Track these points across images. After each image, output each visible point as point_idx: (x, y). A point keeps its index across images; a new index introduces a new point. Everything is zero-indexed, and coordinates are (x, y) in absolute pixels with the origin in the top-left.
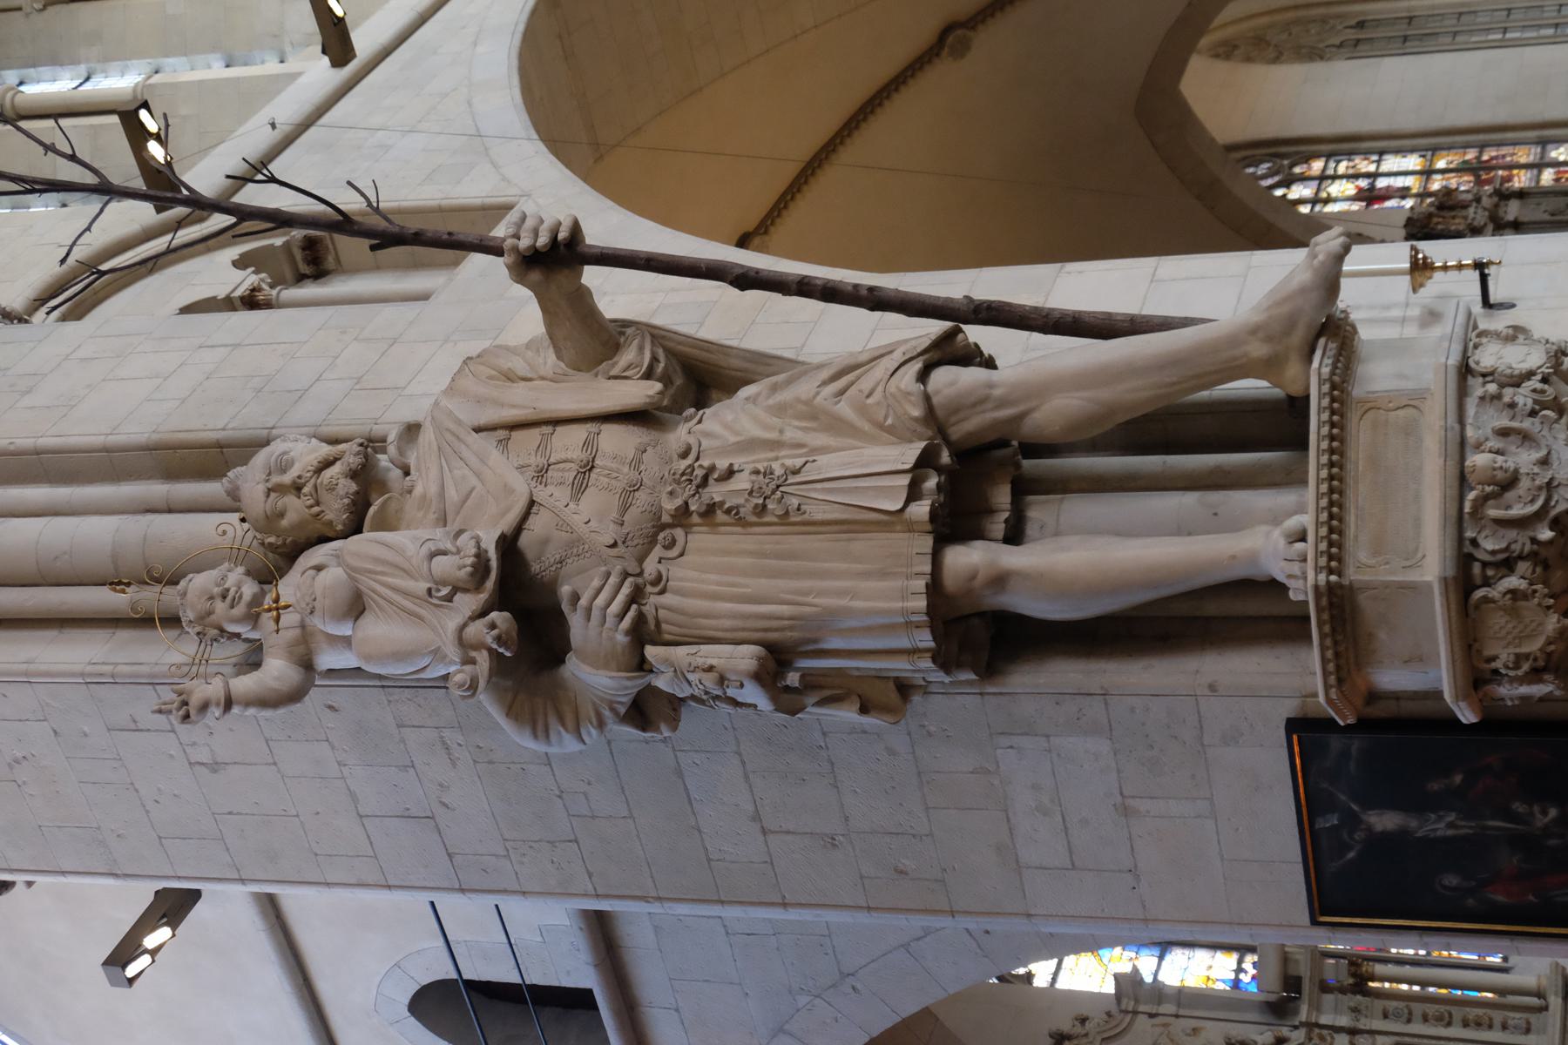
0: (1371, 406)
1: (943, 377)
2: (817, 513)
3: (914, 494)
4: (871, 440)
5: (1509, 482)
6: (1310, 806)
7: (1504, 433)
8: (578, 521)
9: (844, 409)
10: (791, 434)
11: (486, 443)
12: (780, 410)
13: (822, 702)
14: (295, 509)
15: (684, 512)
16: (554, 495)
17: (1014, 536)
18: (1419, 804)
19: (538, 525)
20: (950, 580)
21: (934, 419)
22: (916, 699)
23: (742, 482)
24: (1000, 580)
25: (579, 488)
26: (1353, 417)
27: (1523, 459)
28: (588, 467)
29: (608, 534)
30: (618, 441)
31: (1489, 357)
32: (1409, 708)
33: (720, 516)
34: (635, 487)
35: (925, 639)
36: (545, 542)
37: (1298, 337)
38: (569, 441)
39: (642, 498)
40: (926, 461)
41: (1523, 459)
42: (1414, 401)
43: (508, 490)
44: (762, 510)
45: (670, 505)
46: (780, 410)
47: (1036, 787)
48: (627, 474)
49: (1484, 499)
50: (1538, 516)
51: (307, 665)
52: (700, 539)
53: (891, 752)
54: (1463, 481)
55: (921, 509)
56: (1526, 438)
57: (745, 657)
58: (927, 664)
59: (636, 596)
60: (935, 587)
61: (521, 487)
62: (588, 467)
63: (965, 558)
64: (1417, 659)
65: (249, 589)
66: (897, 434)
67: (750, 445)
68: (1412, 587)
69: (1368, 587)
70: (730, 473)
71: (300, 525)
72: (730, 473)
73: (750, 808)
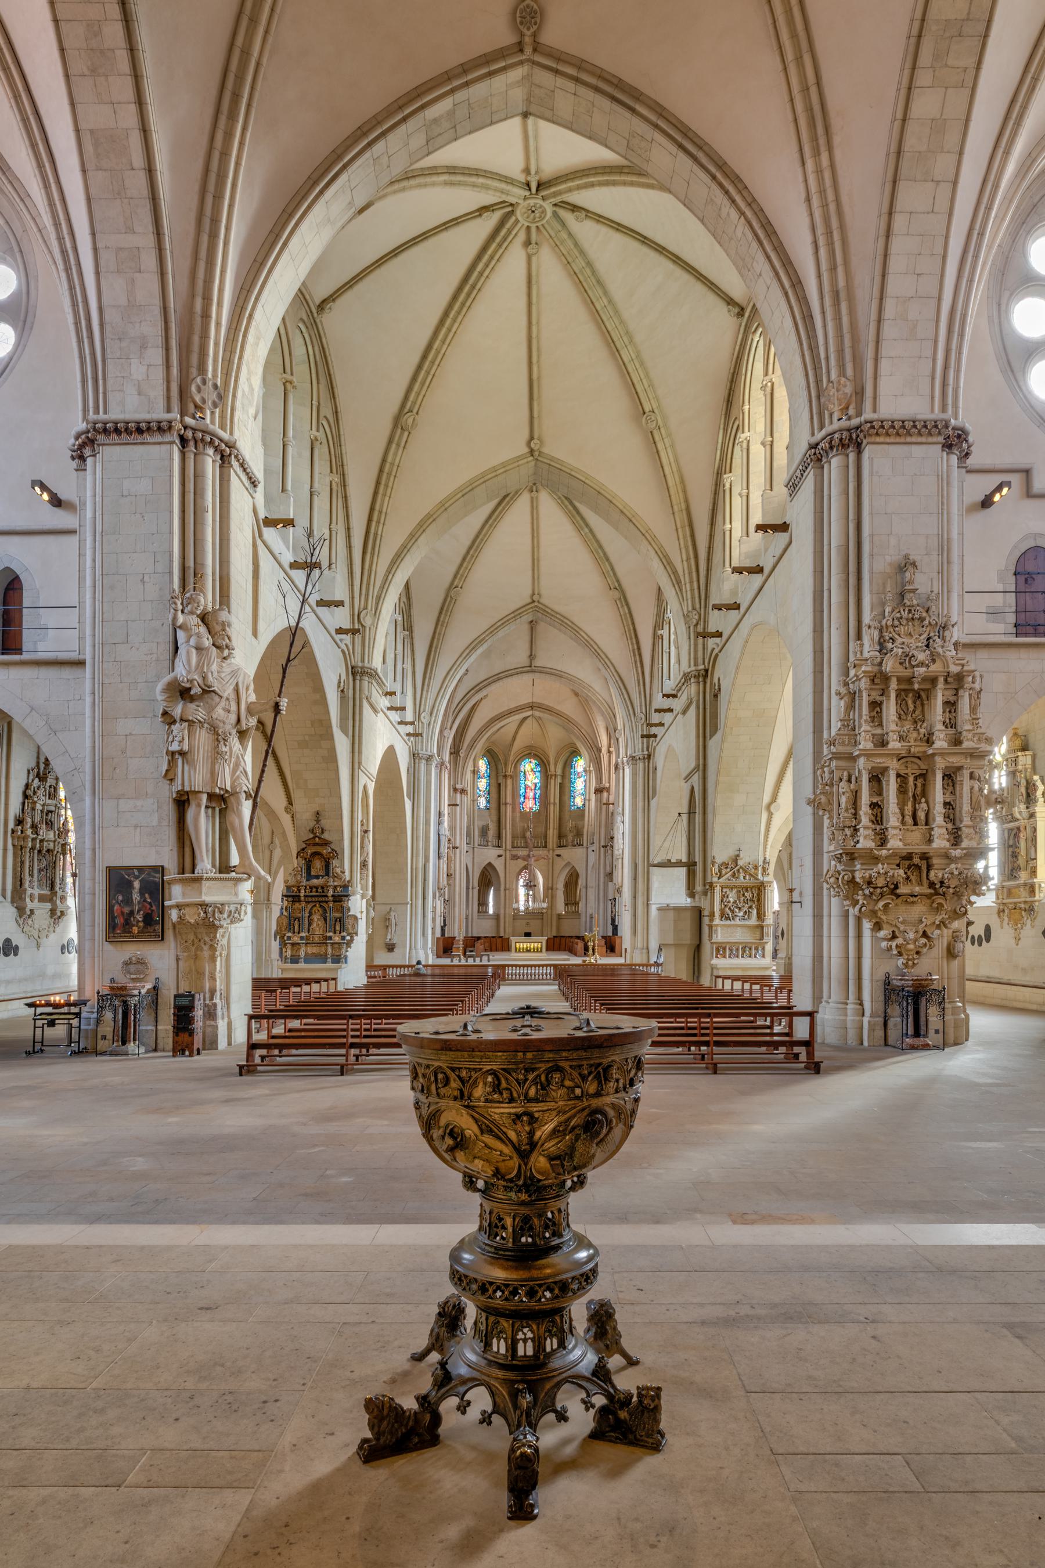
0: (235, 885)
1: (244, 795)
2: (217, 766)
3: (220, 789)
4: (231, 778)
5: (221, 913)
6: (141, 869)
7: (230, 912)
8: (217, 708)
9: (238, 773)
10: (233, 760)
11: (235, 683)
12: (238, 757)
13: (169, 759)
14: (218, 628)
15: (218, 735)
16: (223, 703)
17: (207, 807)
18: (142, 892)
19: (217, 699)
20: (200, 795)
21: (235, 794)
22: (168, 782)
23: (224, 749)
24: (199, 806)
25: (224, 709)
26: (233, 882)
27: (225, 916)
28: (229, 711)
29: (214, 717)
30: (233, 718)
31: (243, 908)
32: (166, 891)
33: (216, 743)
34: (224, 723)
35: (187, 789)
36: (213, 700)
37: (248, 871)
38: (234, 707)
39: (221, 725)
40: (227, 791)
41: (225, 916)
42: (236, 894)
43: (225, 691)
44: (218, 753)
45: (220, 732)
46: (238, 757)
47: (142, 806)
48: (227, 721)
49: (219, 908)
50: (215, 918)
51: (180, 627)
52: (212, 737)
53: (152, 773)
54: (222, 905)
55: (217, 791)
56: (229, 916)
57: (186, 748)
58: (180, 788)
59: (200, 722)
60: (199, 792)
61: (225, 695)
62: (229, 711)
63: (205, 797)
64: (184, 894)
65: (199, 612)
66: (233, 786)
67: (231, 749)
68: (201, 893)
69: (201, 885)
70: (226, 746)
71: (213, 627)
72: (226, 746)
73: (134, 733)
